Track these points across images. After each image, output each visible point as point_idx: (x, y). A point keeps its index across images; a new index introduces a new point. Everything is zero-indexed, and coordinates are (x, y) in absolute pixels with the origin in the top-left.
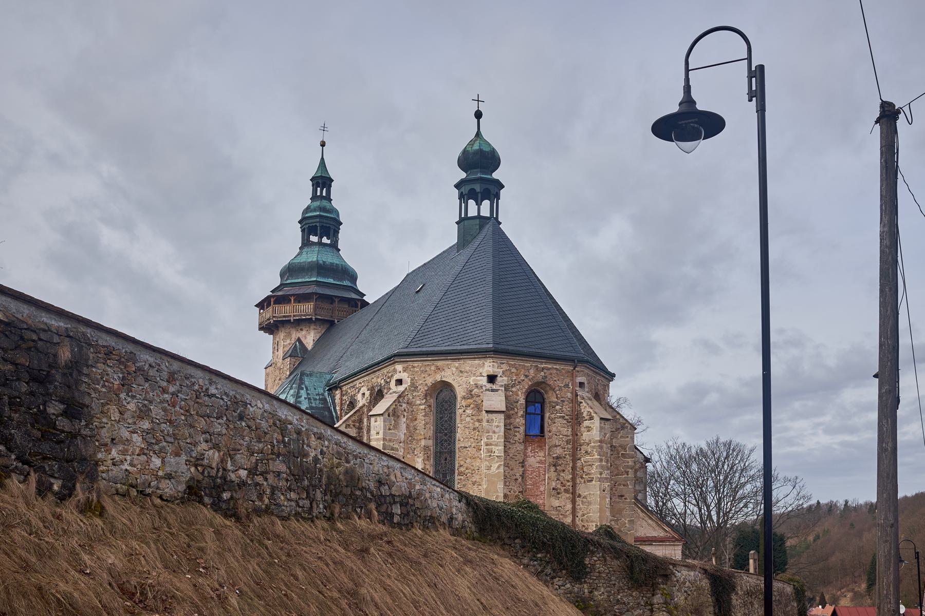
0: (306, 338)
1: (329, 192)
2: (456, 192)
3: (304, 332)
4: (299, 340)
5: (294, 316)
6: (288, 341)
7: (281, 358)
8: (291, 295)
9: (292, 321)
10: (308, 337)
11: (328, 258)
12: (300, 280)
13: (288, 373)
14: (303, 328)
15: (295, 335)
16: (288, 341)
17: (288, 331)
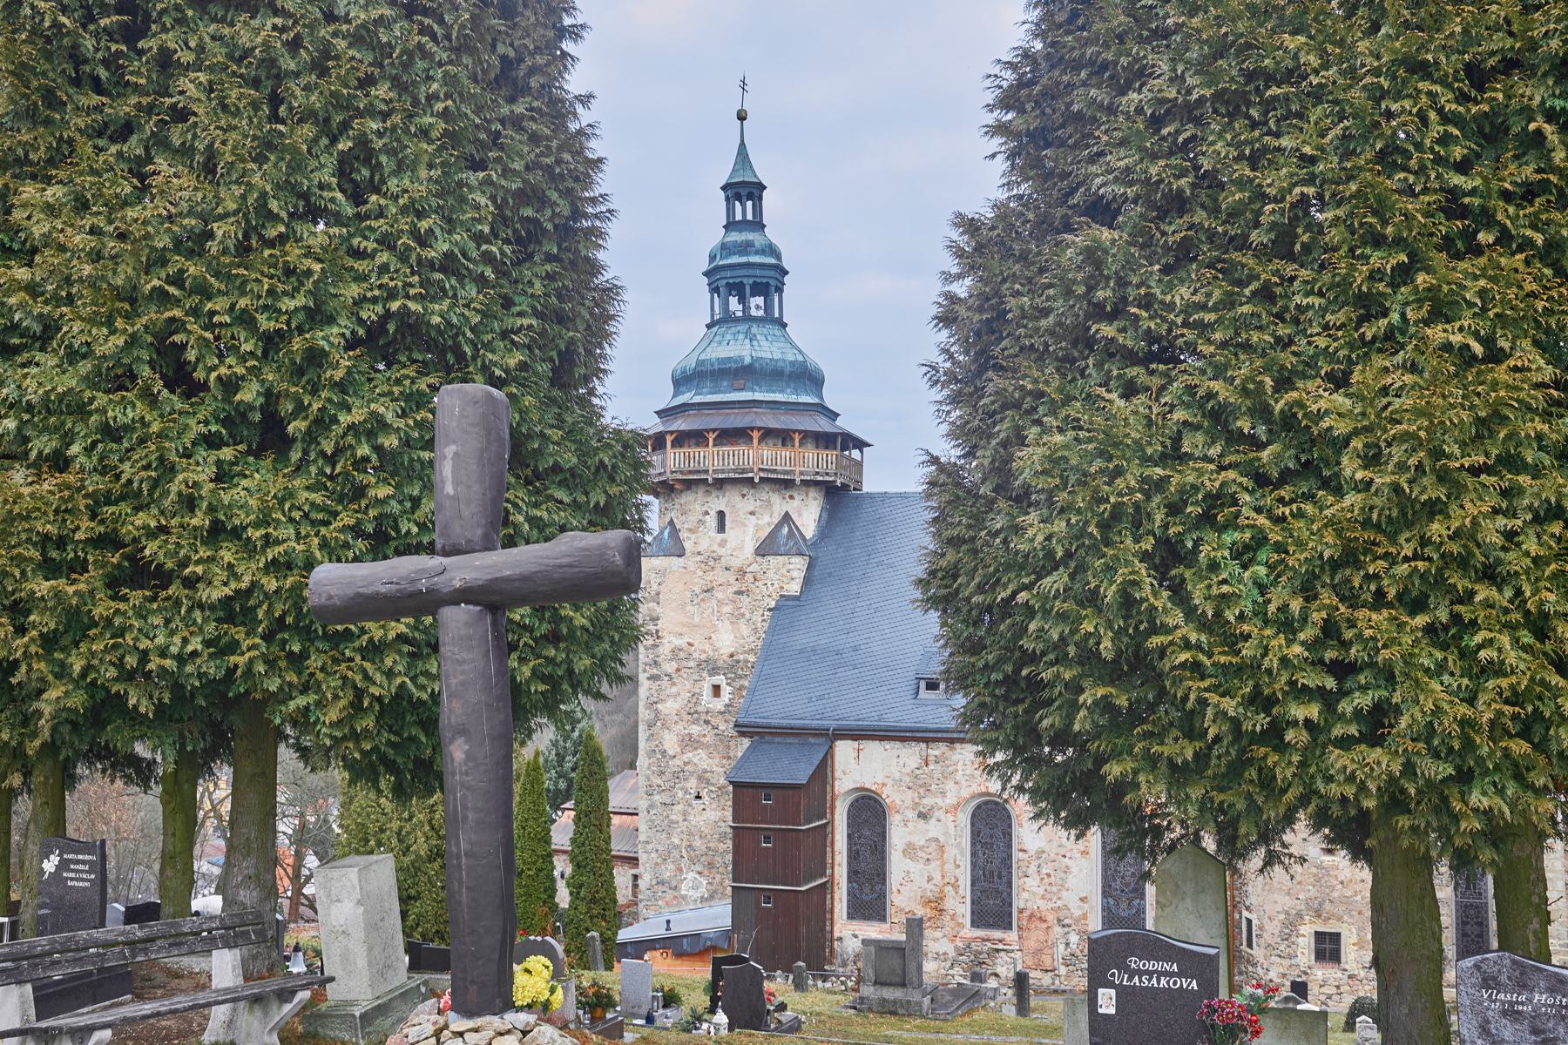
0: (800, 515)
1: (758, 210)
2: (722, 194)
3: (796, 503)
4: (787, 518)
5: (801, 473)
6: (766, 519)
7: (750, 547)
8: (794, 431)
9: (798, 482)
10: (805, 514)
11: (767, 348)
12: (779, 397)
13: (794, 588)
14: (795, 495)
15: (780, 504)
16: (766, 519)
17: (765, 496)
